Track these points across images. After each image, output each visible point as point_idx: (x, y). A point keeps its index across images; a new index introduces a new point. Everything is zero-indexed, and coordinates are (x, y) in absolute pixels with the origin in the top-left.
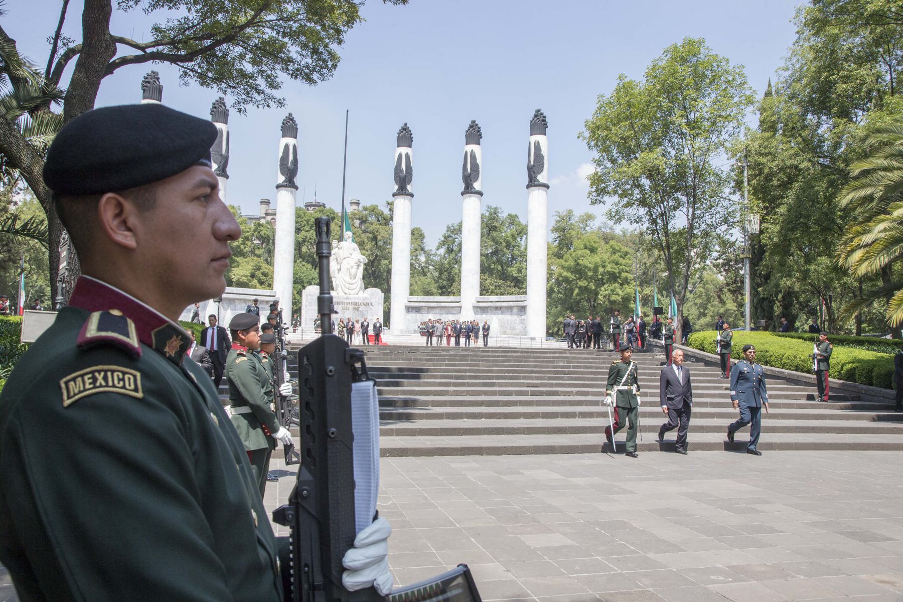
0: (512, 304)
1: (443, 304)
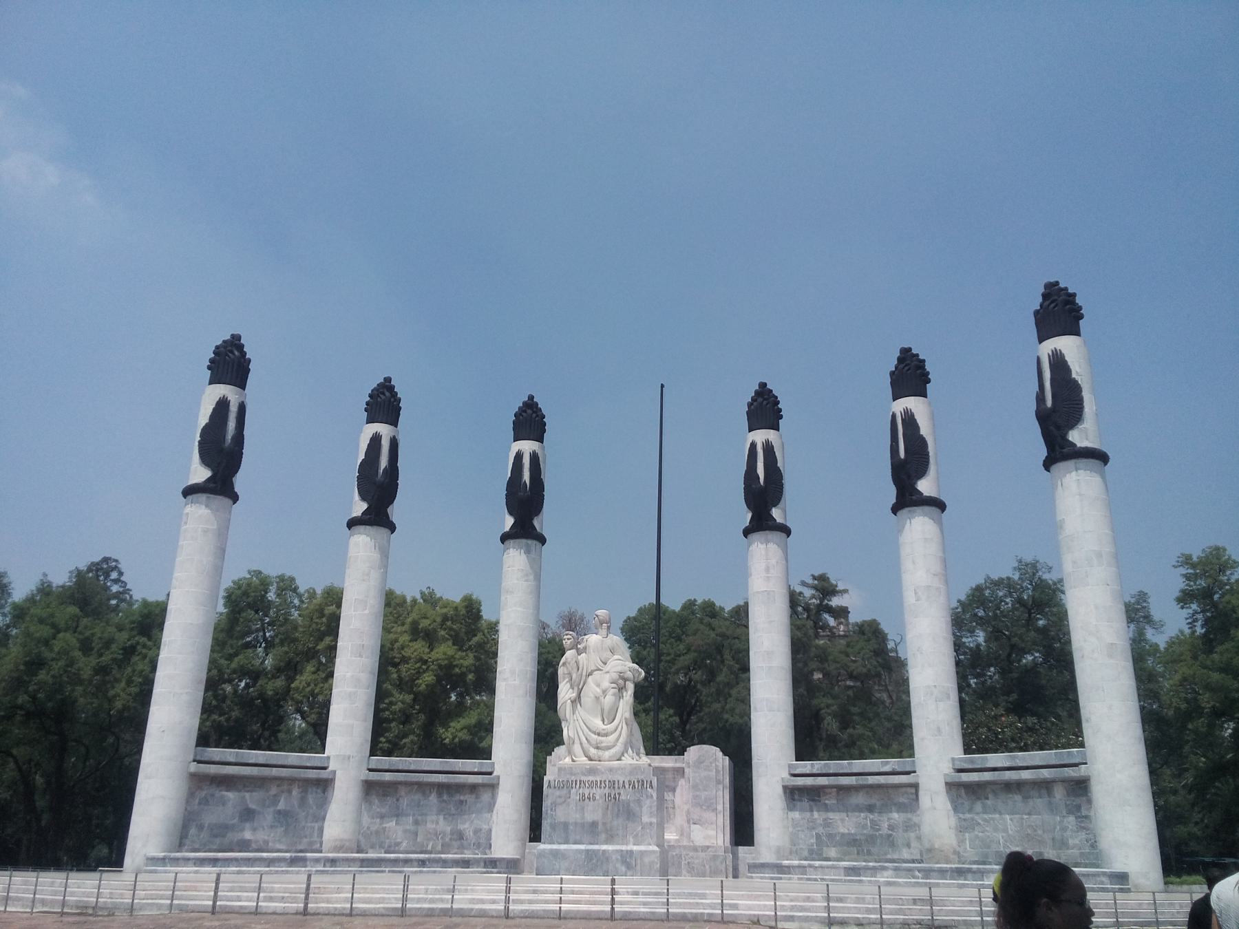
0: (1046, 774)
1: (871, 780)
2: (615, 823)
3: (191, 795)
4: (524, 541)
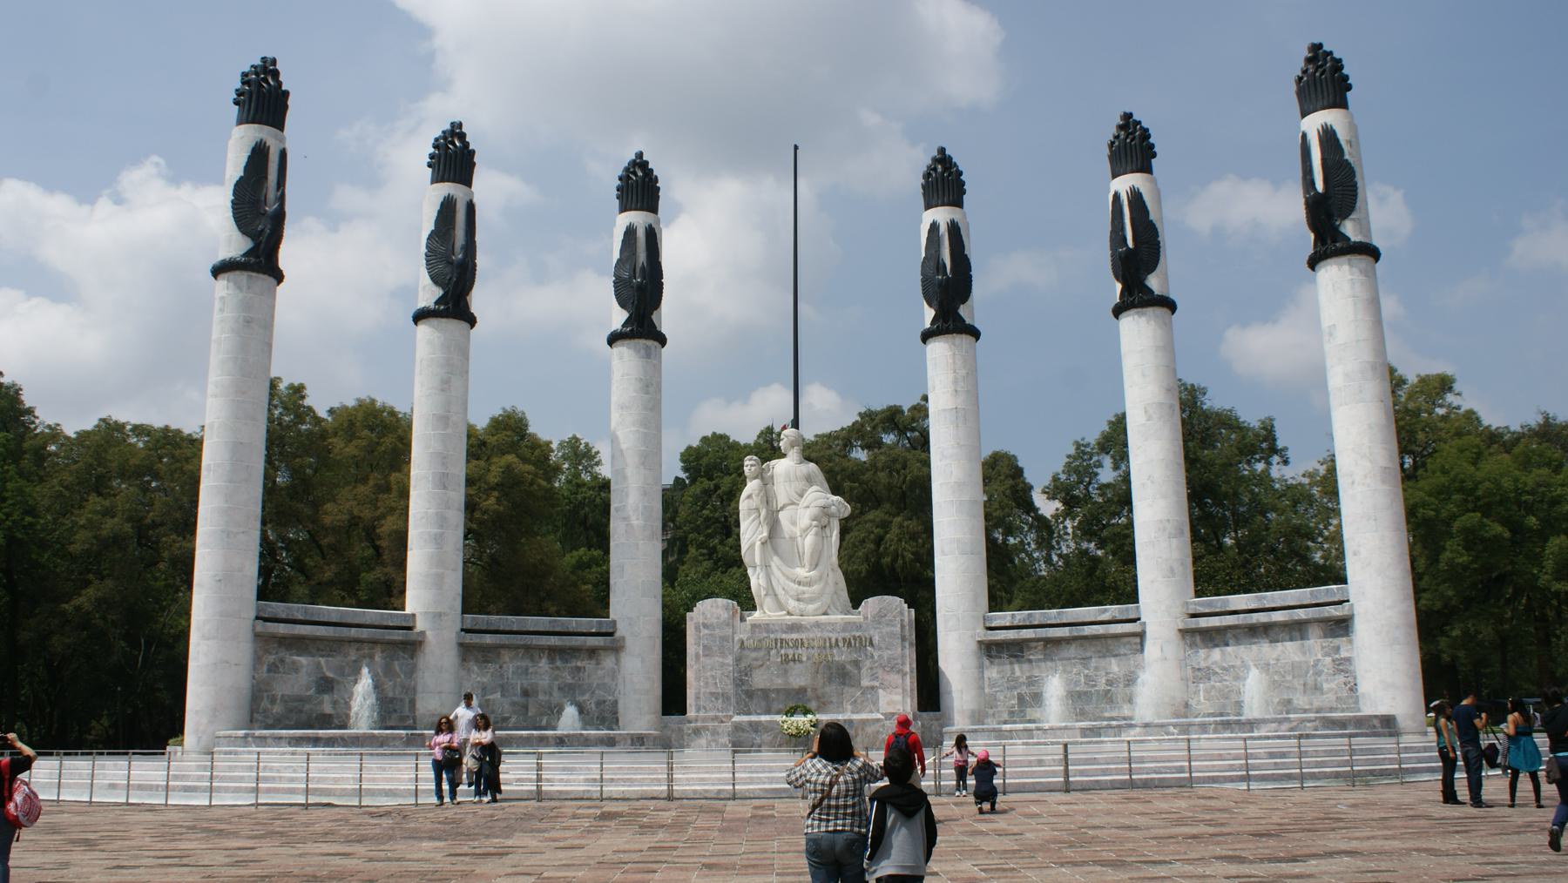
0: (1301, 614)
1: (1088, 630)
2: (828, 689)
3: (257, 660)
4: (642, 342)
